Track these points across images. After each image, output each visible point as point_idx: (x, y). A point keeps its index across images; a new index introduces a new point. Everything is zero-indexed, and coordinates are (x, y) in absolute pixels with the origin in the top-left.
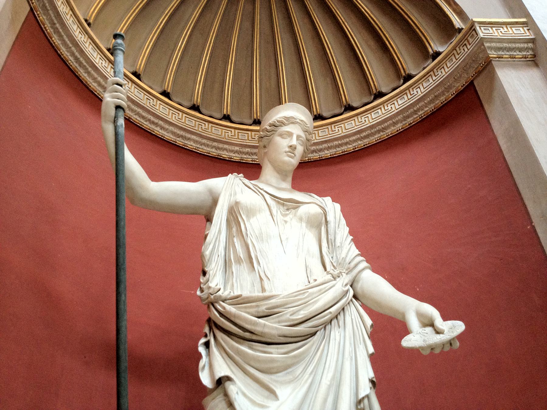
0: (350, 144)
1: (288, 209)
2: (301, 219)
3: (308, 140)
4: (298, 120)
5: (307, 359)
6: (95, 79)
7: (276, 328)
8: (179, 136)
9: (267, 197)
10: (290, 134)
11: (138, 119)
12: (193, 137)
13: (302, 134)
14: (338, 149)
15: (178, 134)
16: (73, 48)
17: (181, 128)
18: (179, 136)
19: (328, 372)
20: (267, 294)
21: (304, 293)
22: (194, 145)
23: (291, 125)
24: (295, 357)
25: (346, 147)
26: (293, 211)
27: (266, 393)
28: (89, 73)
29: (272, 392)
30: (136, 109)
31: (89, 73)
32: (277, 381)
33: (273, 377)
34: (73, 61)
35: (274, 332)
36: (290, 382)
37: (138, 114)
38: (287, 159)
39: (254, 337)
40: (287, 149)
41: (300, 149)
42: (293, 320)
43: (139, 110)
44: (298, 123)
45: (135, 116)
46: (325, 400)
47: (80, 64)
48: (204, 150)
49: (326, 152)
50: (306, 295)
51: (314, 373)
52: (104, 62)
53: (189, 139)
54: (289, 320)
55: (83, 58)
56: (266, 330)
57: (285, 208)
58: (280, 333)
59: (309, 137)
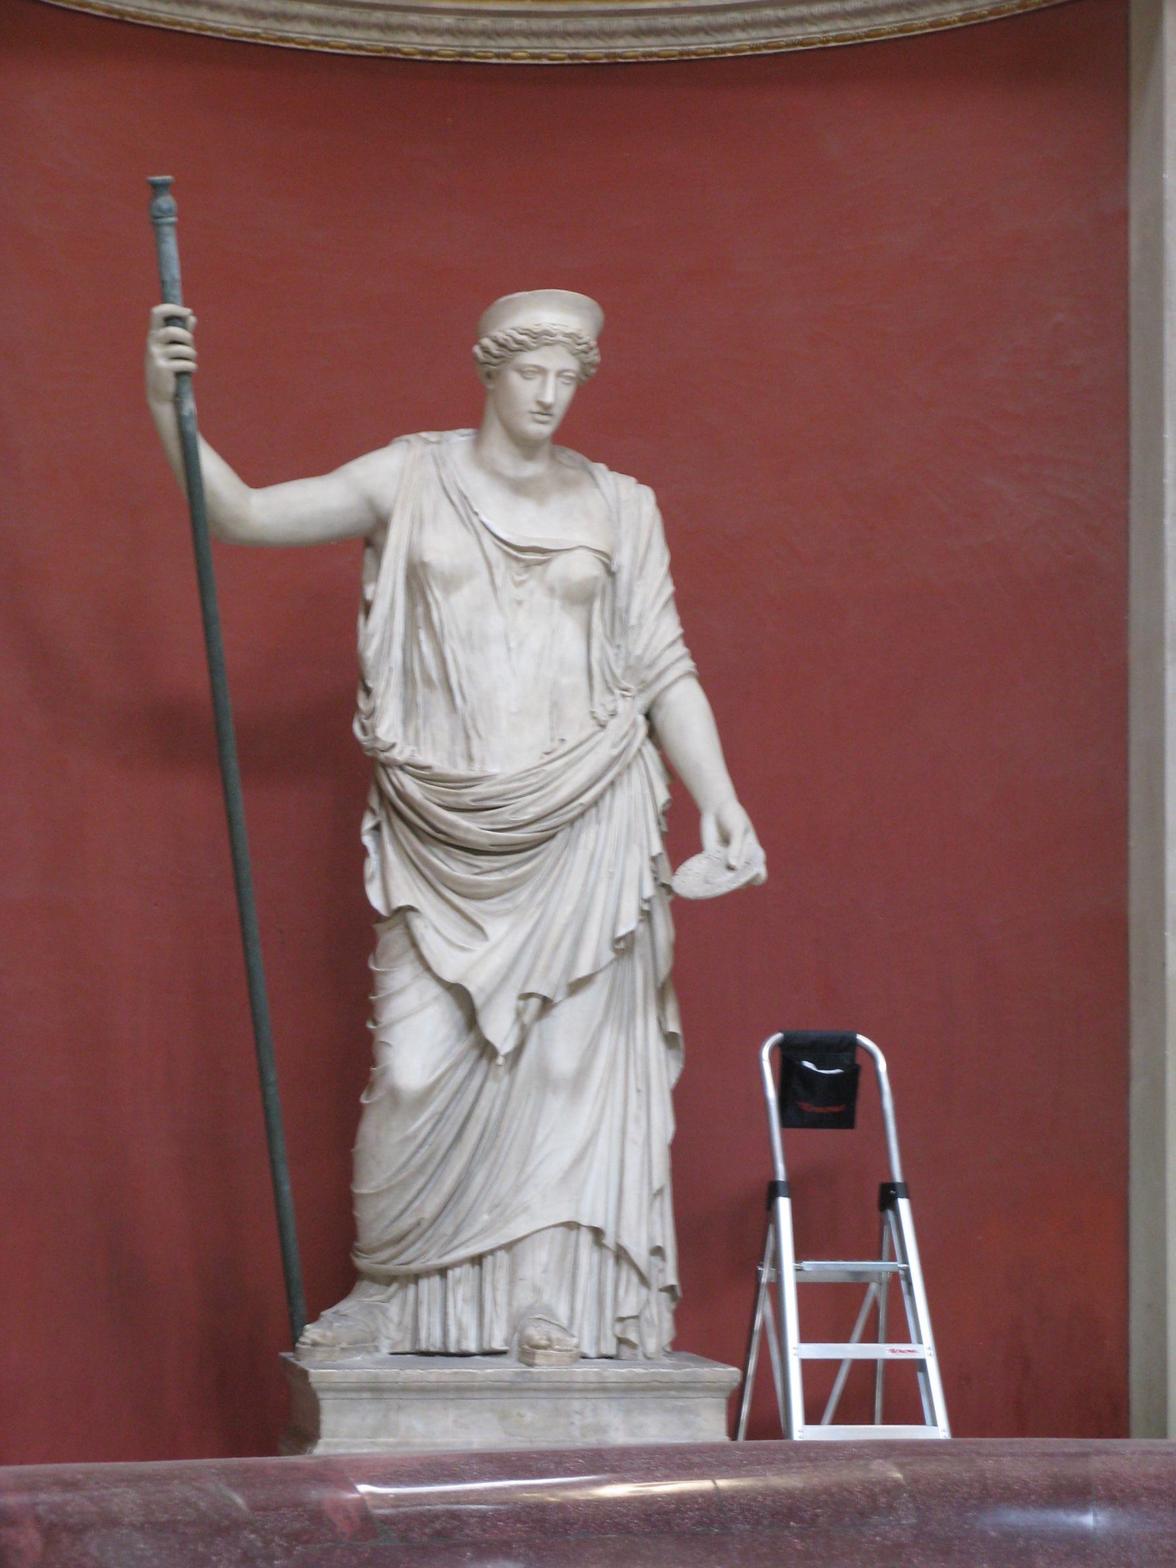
2: (552, 591)
4: (560, 338)
5: (537, 878)
9: (487, 540)
10: (542, 371)
20: (476, 772)
27: (470, 928)
29: (480, 928)
32: (487, 913)
33: (481, 905)
36: (507, 913)
40: (535, 408)
50: (541, 776)
57: (522, 564)
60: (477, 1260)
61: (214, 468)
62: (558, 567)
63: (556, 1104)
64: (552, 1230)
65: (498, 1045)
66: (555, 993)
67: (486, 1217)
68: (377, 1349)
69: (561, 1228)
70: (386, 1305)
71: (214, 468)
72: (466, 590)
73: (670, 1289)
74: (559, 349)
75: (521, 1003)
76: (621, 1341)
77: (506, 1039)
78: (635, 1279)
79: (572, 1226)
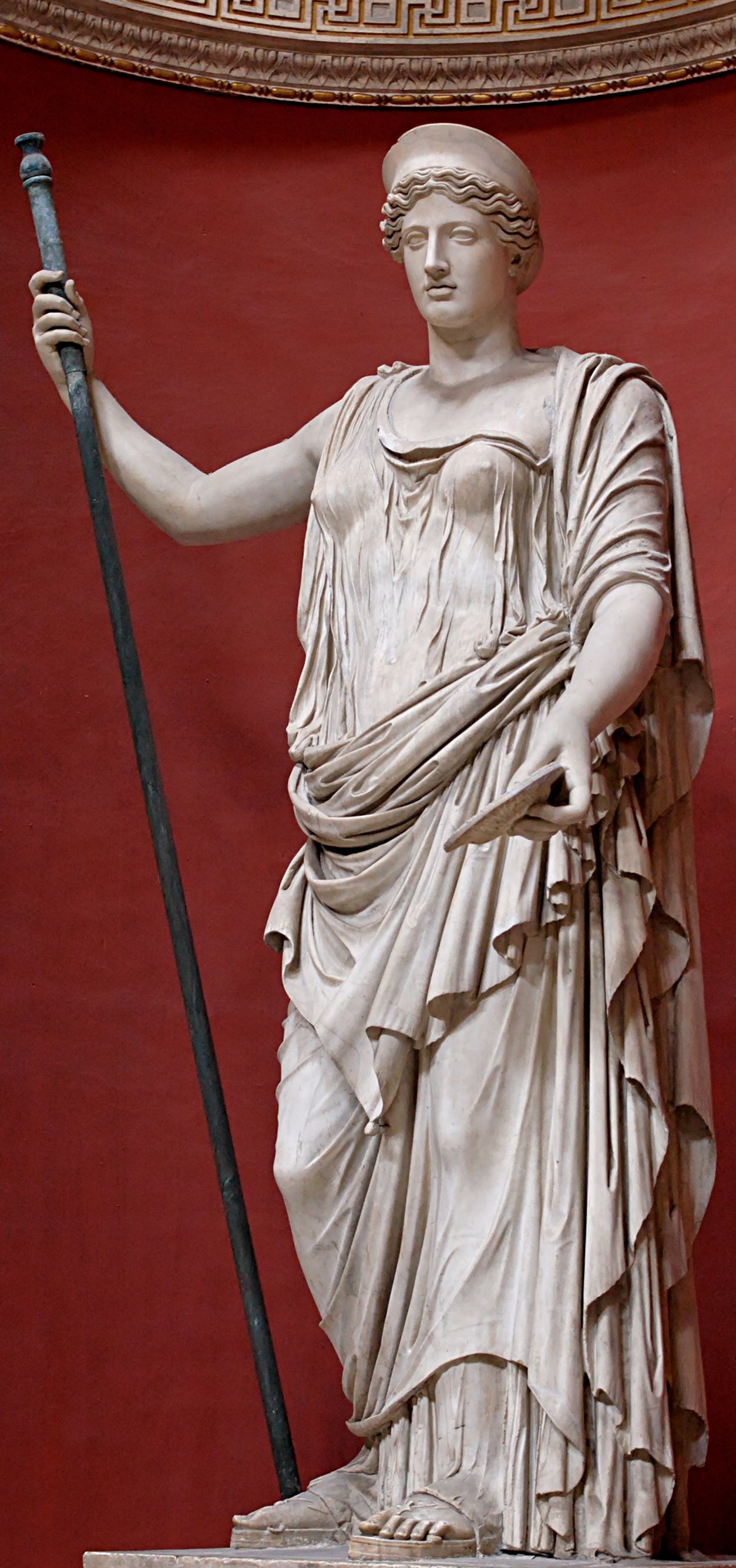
1: (421, 479)
4: (432, 182)
5: (408, 874)
6: (232, 61)
8: (548, 70)
12: (593, 49)
15: (544, 67)
16: (128, 27)
17: (543, 45)
18: (548, 70)
19: (419, 901)
21: (384, 729)
22: (606, 73)
23: (421, 203)
28: (206, 56)
30: (388, 62)
31: (206, 56)
32: (353, 929)
33: (353, 920)
34: (148, 56)
37: (400, 74)
41: (465, 258)
44: (431, 189)
45: (395, 86)
47: (170, 50)
48: (644, 72)
51: (404, 905)
53: (582, 64)
55: (170, 30)
58: (347, 830)
66: (423, 1029)
69: (478, 1365)
72: (358, 526)
75: (375, 1043)
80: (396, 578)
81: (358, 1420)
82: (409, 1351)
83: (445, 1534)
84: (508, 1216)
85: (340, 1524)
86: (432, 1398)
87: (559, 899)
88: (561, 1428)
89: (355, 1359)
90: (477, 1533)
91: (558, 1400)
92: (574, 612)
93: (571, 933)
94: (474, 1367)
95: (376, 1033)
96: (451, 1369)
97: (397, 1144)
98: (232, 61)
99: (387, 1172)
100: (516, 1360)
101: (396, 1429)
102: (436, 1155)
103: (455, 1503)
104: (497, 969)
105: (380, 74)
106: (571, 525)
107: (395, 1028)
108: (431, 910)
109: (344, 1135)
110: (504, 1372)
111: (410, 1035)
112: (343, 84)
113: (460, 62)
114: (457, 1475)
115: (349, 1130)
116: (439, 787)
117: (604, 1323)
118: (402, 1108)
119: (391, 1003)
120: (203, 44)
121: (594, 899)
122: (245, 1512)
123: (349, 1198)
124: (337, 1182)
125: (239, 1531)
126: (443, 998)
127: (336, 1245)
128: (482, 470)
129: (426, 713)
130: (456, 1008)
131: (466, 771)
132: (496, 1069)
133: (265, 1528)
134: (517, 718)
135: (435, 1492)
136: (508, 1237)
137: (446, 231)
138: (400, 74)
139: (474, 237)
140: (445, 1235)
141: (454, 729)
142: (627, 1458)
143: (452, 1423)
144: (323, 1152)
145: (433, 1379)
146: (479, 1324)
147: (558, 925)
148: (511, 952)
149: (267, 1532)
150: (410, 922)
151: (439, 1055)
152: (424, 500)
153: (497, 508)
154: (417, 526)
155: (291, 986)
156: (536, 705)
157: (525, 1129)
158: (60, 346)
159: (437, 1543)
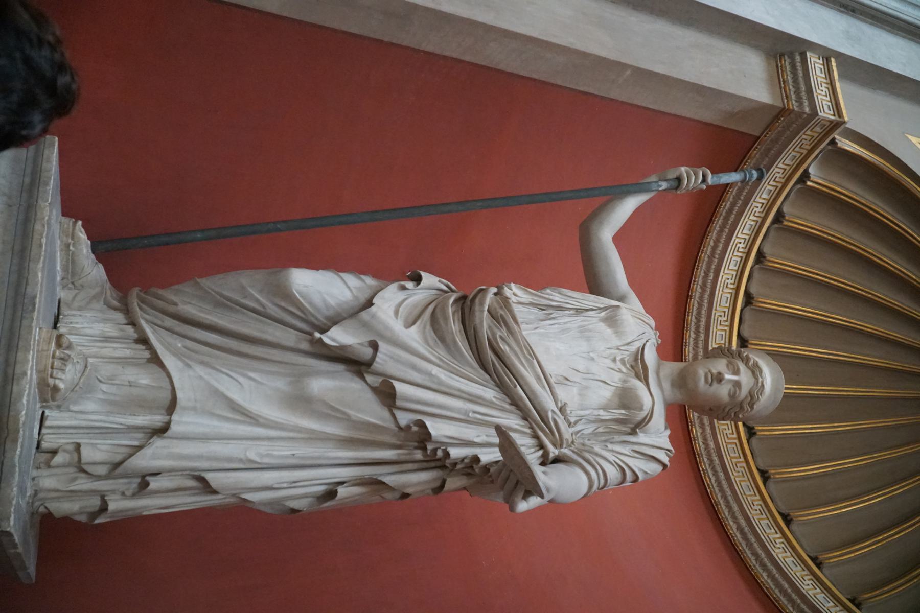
0: (793, 607)
1: (632, 366)
2: (625, 381)
3: (742, 407)
4: (760, 379)
6: (717, 241)
7: (482, 322)
11: (695, 308)
13: (744, 391)
14: (777, 591)
23: (750, 373)
24: (455, 342)
25: (786, 602)
26: (633, 374)
28: (721, 231)
29: (414, 323)
31: (721, 231)
32: (424, 328)
33: (428, 327)
35: (477, 321)
37: (700, 306)
38: (701, 373)
39: (467, 311)
40: (714, 371)
41: (723, 392)
42: (496, 339)
43: (705, 306)
44: (757, 379)
46: (414, 367)
47: (726, 218)
49: (764, 575)
51: (441, 364)
52: (742, 245)
54: (494, 335)
56: (477, 314)
57: (633, 364)
59: (746, 407)
60: (143, 341)
61: (628, 206)
62: (639, 385)
63: (281, 384)
64: (169, 387)
65: (329, 333)
67: (180, 345)
68: (64, 287)
70: (102, 303)
71: (628, 206)
72: (609, 331)
73: (104, 508)
74: (753, 380)
75: (367, 344)
76: (54, 452)
77: (333, 340)
78: (118, 458)
79: (172, 406)
80: (591, 354)
81: (138, 296)
82: (180, 345)
83: (56, 389)
84: (261, 421)
85: (73, 283)
86: (149, 361)
87: (440, 453)
88: (125, 464)
89: (176, 304)
90: (56, 403)
91: (143, 461)
92: (573, 451)
93: (418, 455)
94: (167, 395)
95: (374, 346)
96: (167, 379)
97: (305, 346)
98: (717, 241)
99: (289, 337)
100: (172, 425)
101: (130, 330)
102: (299, 376)
103: (77, 388)
104: (404, 418)
105: (701, 297)
106: (610, 446)
107: (377, 359)
108: (441, 383)
109: (310, 312)
110: (163, 412)
111: (372, 367)
112: (700, 283)
113: (702, 329)
114: (97, 381)
115: (313, 316)
116: (501, 386)
117: (192, 483)
118: (325, 351)
119: (391, 357)
120: (727, 230)
121: (433, 464)
122: (83, 226)
123: (272, 310)
124: (283, 304)
125: (71, 224)
126: (393, 388)
127: (245, 297)
128: (642, 405)
129: (538, 378)
130: (387, 395)
131: (508, 400)
132: (348, 416)
133: (73, 239)
134: (531, 428)
135: (86, 374)
136: (248, 420)
137: (737, 384)
138: (700, 306)
139: (732, 396)
140: (251, 378)
141: (531, 397)
142: (103, 498)
143: (132, 379)
144: (301, 299)
145: (161, 365)
146: (196, 401)
147: (424, 449)
148: (415, 428)
149: (70, 241)
150: (435, 370)
151: (357, 379)
152: (624, 370)
153: (623, 412)
154: (612, 365)
155: (393, 287)
156: (536, 437)
157: (313, 431)
158: (679, 180)
159: (48, 385)
